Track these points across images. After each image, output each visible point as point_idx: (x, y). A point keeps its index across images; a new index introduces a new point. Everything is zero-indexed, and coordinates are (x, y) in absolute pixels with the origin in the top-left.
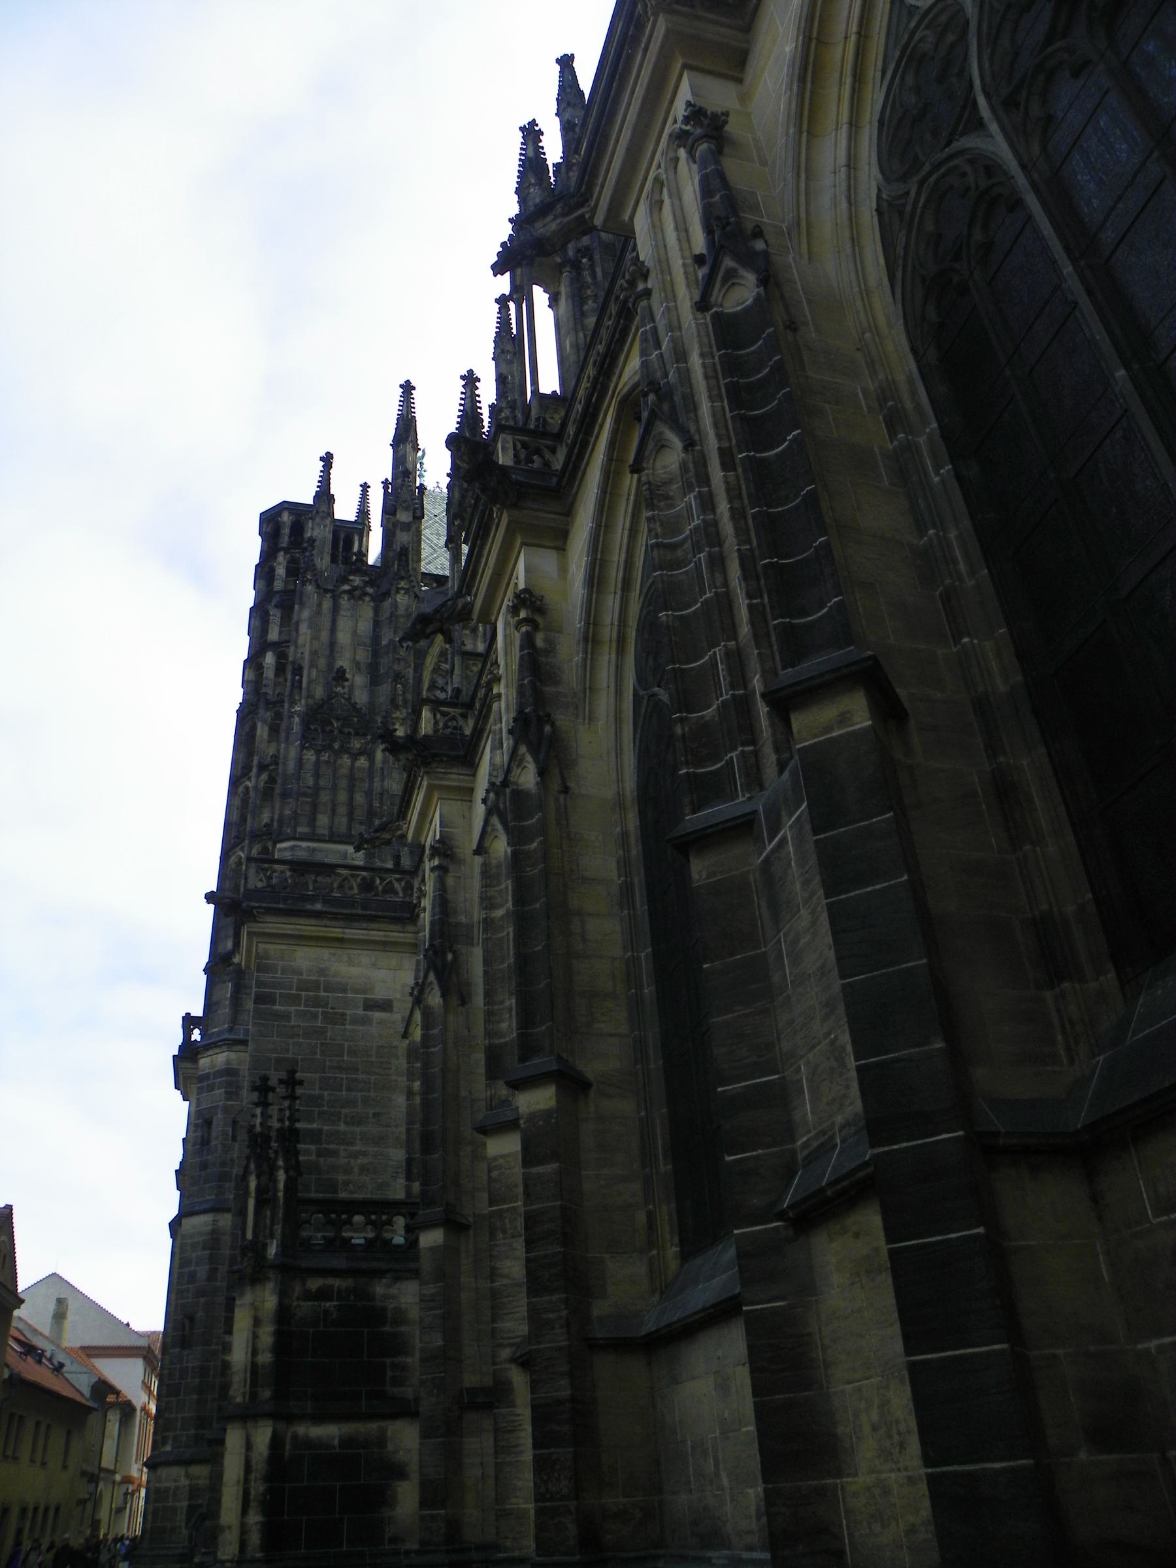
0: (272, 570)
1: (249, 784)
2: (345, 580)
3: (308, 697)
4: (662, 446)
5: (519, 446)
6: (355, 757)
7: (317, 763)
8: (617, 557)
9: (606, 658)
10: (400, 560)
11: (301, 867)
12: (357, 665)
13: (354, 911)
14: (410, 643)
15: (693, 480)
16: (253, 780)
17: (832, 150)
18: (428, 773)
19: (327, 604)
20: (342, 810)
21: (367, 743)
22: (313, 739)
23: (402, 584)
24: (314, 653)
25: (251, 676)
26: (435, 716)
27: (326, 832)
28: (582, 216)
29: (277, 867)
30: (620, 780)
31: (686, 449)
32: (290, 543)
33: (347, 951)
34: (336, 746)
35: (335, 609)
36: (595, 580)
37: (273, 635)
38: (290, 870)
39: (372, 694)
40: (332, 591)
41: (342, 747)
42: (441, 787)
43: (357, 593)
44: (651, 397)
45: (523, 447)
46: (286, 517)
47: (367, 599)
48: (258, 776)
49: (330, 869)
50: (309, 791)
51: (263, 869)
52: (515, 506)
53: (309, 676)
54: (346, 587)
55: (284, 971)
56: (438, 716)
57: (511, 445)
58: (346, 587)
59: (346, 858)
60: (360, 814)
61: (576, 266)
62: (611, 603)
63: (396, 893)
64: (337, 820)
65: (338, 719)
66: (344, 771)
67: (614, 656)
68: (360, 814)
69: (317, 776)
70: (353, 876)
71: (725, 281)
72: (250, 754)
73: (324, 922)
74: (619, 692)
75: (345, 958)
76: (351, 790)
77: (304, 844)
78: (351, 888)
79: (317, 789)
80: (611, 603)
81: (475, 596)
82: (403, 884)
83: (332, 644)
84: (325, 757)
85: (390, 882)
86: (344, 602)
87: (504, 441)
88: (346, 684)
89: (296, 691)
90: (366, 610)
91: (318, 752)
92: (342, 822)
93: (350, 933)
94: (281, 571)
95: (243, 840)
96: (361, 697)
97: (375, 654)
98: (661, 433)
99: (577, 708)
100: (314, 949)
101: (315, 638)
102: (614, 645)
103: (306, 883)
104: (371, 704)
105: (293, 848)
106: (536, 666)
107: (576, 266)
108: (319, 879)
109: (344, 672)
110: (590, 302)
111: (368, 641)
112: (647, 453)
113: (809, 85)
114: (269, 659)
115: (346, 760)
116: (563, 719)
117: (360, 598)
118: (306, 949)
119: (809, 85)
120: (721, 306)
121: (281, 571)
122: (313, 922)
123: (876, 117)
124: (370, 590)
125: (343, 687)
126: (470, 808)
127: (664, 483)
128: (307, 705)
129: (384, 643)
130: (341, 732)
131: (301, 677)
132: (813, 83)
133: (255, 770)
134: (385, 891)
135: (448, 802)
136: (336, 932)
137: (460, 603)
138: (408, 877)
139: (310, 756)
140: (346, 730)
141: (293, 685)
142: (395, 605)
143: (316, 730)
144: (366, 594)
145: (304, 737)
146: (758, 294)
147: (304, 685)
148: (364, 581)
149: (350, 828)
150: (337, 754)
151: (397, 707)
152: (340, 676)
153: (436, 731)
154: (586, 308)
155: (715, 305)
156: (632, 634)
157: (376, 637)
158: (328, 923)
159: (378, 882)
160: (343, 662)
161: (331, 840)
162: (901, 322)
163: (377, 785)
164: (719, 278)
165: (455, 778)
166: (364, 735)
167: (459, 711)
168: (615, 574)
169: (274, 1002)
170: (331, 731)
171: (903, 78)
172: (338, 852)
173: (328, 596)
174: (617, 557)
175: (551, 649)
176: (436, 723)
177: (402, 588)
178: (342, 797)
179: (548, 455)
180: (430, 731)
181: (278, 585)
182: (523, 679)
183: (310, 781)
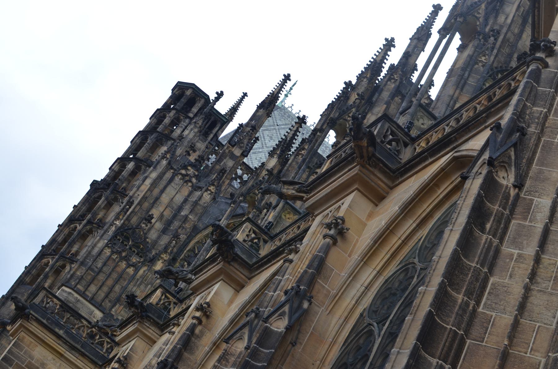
0: (164, 117)
1: (78, 225)
2: (185, 167)
3: (127, 219)
4: (240, 339)
6: (129, 266)
7: (109, 258)
10: (219, 174)
11: (65, 307)
12: (162, 216)
13: (76, 345)
14: (159, 276)
15: (238, 363)
16: (81, 226)
17: (367, 275)
18: (140, 322)
19: (169, 175)
20: (105, 289)
21: (139, 262)
22: (115, 244)
23: (212, 188)
24: (145, 198)
25: (116, 168)
26: (162, 295)
27: (90, 295)
28: (304, 197)
29: (55, 300)
31: (246, 348)
32: (183, 108)
33: (61, 362)
34: (124, 254)
35: (171, 180)
37: (140, 154)
38: (60, 306)
39: (159, 237)
40: (175, 170)
41: (126, 256)
43: (187, 178)
44: (253, 315)
46: (189, 92)
47: (190, 184)
48: (85, 226)
49: (80, 317)
50: (96, 270)
51: (48, 297)
53: (134, 209)
54: (183, 172)
55: (25, 353)
56: (163, 297)
58: (183, 172)
59: (91, 314)
60: (113, 296)
63: (103, 347)
64: (100, 292)
65: (133, 241)
66: (119, 269)
68: (113, 296)
69: (105, 264)
70: (87, 327)
71: (279, 315)
72: (89, 210)
73: (59, 342)
75: (58, 365)
76: (117, 282)
77: (76, 295)
78: (84, 332)
79: (100, 271)
81: (196, 279)
82: (109, 346)
83: (157, 199)
84: (114, 257)
85: (104, 341)
86: (177, 179)
87: (246, 227)
88: (149, 225)
89: (123, 213)
90: (186, 191)
91: (113, 253)
92: (101, 295)
93: (68, 355)
94: (167, 121)
95: (56, 255)
96: (153, 235)
97: (175, 216)
98: (244, 333)
100: (46, 351)
101: (150, 190)
103: (64, 317)
104: (155, 242)
105: (70, 293)
108: (71, 318)
109: (152, 218)
111: (175, 207)
112: (234, 337)
113: (377, 245)
114: (131, 166)
115: (123, 264)
117: (186, 182)
118: (43, 349)
119: (377, 245)
120: (271, 325)
121: (167, 121)
122: (54, 338)
123: (386, 278)
124: (194, 180)
125: (147, 226)
126: (149, 349)
127: (231, 354)
128: (124, 223)
129: (182, 213)
130: (130, 249)
131: (130, 207)
132: (379, 245)
133: (85, 221)
134: (97, 343)
135: (140, 340)
136: (62, 349)
137: (190, 276)
138: (113, 344)
139: (108, 252)
140: (133, 249)
141: (123, 209)
142: (200, 198)
143: (119, 240)
144: (190, 181)
145: (110, 240)
146: (283, 331)
147: (128, 213)
148: (194, 173)
149: (103, 300)
150: (122, 259)
151: (166, 252)
152: (149, 218)
153: (157, 304)
155: (269, 323)
157: (180, 208)
158: (61, 343)
159: (98, 337)
160: (156, 212)
161: (89, 302)
162: (331, 366)
163: (130, 286)
164: (279, 313)
166: (141, 257)
167: (175, 300)
169: (11, 365)
170: (126, 245)
171: (401, 273)
172: (89, 309)
173: (172, 171)
175: (199, 337)
176: (160, 300)
177: (210, 190)
178: (110, 282)
179: (261, 243)
180: (154, 303)
183: (99, 265)
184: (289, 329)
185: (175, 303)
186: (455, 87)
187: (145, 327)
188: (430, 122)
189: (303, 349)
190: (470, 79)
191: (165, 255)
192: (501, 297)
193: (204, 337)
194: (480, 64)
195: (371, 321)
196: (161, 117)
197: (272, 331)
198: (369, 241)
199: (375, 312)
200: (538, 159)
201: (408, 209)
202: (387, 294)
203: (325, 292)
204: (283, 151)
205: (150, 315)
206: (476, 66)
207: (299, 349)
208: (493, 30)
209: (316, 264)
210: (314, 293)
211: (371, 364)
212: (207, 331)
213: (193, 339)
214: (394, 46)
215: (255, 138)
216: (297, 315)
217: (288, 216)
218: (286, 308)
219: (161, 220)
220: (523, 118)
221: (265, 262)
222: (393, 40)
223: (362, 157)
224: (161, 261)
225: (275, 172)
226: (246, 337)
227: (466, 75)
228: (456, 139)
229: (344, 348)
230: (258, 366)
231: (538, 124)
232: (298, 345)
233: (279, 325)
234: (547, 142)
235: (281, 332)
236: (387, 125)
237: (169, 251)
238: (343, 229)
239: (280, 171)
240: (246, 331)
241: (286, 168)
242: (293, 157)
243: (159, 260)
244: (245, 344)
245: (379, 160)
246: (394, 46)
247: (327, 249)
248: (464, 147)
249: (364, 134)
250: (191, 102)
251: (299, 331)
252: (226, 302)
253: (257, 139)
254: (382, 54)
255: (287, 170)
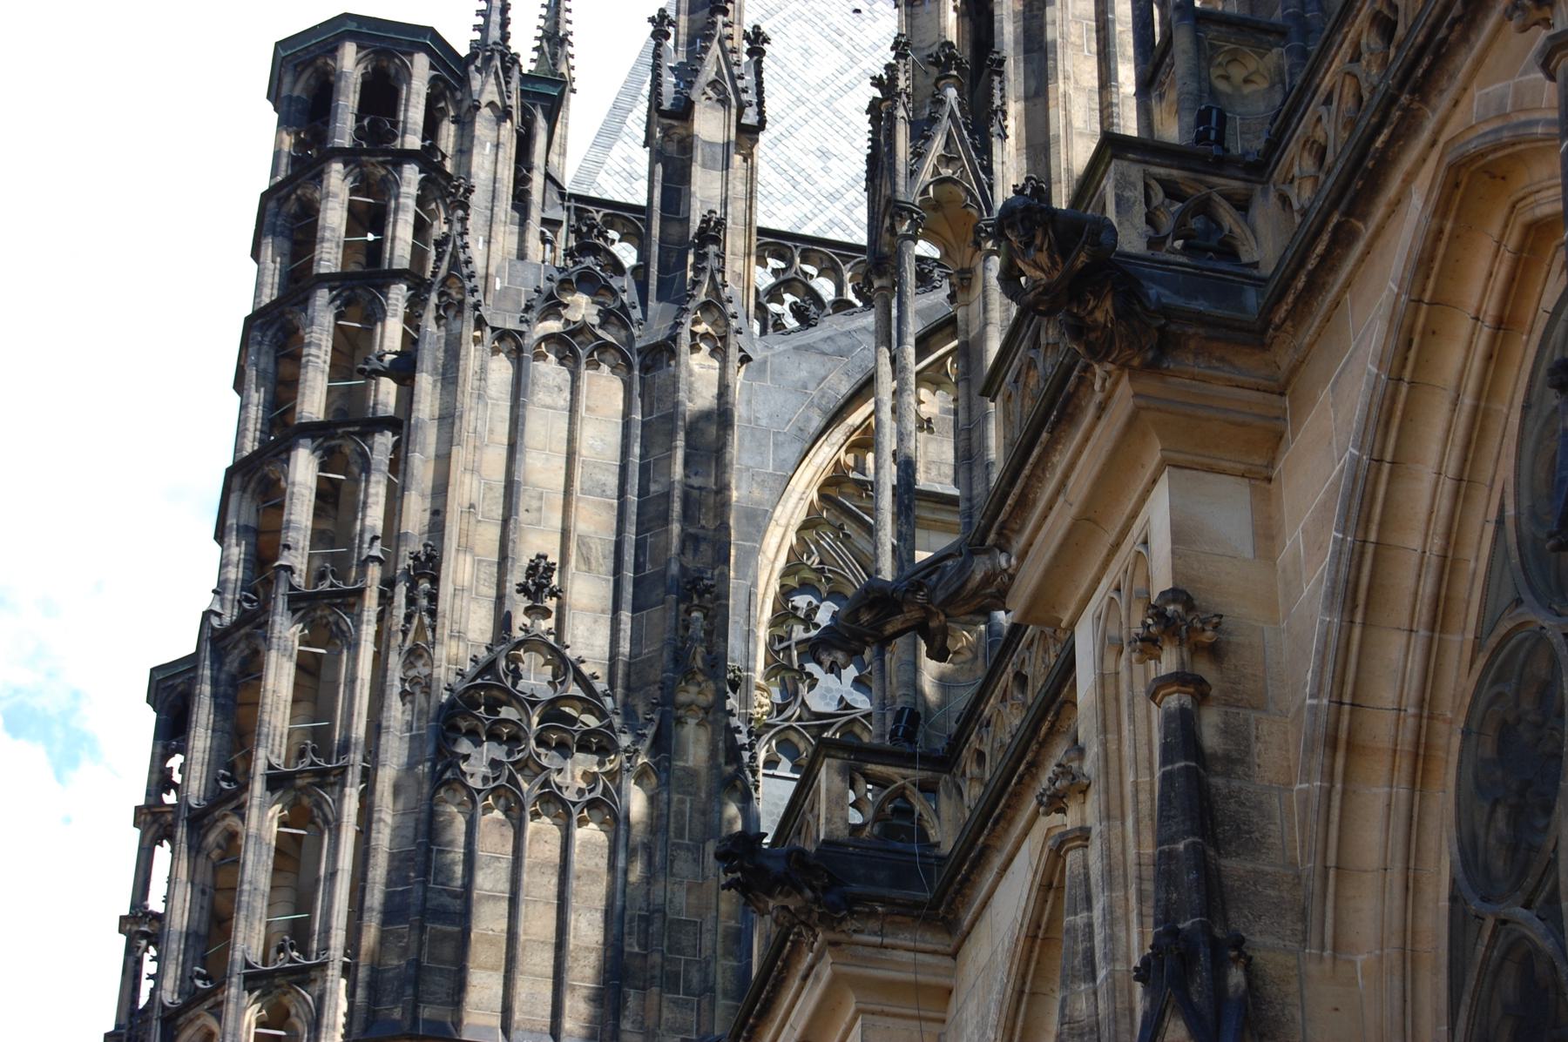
5: (1158, 195)
8: (1416, 541)
9: (1378, 795)
18: (834, 944)
36: (1358, 593)
42: (859, 984)
45: (1168, 195)
52: (1152, 368)
54: (553, 326)
57: (1138, 194)
58: (553, 326)
62: (1396, 656)
67: (1403, 792)
74: (1411, 887)
80: (1396, 656)
81: (1022, 557)
87: (1122, 184)
94: (334, 217)
99: (1303, 916)
102: (1404, 764)
106: (1201, 799)
114: (304, 469)
116: (1269, 944)
121: (334, 217)
137: (980, 568)
151: (688, 674)
156: (1449, 742)
165: (906, 955)
168: (1409, 582)
174: (1416, 541)
175: (1237, 760)
181: (329, 258)
182: (1173, 840)
185: (928, 789)
187: (867, 952)
191: (693, 689)
193: (1257, 747)
196: (295, 217)
205: (856, 888)
212: (1253, 715)
213: (1218, 781)
215: (746, 36)
217: (1237, 73)
219: (587, 561)
221: (1323, 258)
224: (692, 722)
237: (699, 663)
243: (680, 722)
250: (381, 96)
252: (1248, 552)
253: (757, 40)
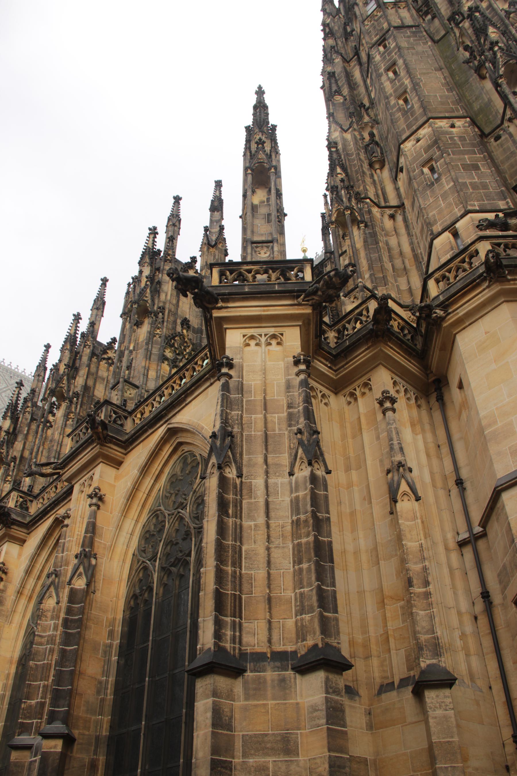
4: (50, 596)
9: (23, 601)
17: (128, 525)
30: (13, 651)
44: (54, 576)
61: (71, 402)
71: (78, 576)
74: (24, 616)
80: (31, 582)
87: (14, 495)
99: (7, 617)
107: (71, 402)
110: (71, 420)
154: (68, 422)
184: (88, 585)
186: (145, 359)
188: (135, 391)
189: (101, 593)
190: (153, 349)
192: (253, 559)
194: (157, 336)
195: (144, 560)
197: (76, 590)
198: (122, 500)
199: (144, 551)
200: (246, 451)
201: (145, 470)
202: (148, 536)
203: (103, 546)
204: (12, 413)
206: (155, 338)
207: (98, 594)
208: (160, 308)
209: (91, 529)
210: (96, 550)
211: (156, 594)
214: (81, 319)
216: (90, 572)
218: (81, 569)
220: (228, 423)
222: (79, 314)
223: (99, 439)
225: (11, 430)
226: (54, 594)
227: (150, 347)
228: (166, 415)
229: (129, 583)
230: (75, 619)
231: (238, 424)
232: (97, 592)
233: (80, 584)
234: (247, 436)
235: (84, 589)
236: (109, 408)
238: (101, 496)
239: (15, 429)
240: (52, 589)
241: (18, 426)
242: (21, 416)
244: (55, 600)
245: (112, 437)
246: (81, 319)
247: (94, 515)
248: (174, 420)
249: (98, 424)
251: (95, 582)
254: (74, 328)
255: (20, 427)
